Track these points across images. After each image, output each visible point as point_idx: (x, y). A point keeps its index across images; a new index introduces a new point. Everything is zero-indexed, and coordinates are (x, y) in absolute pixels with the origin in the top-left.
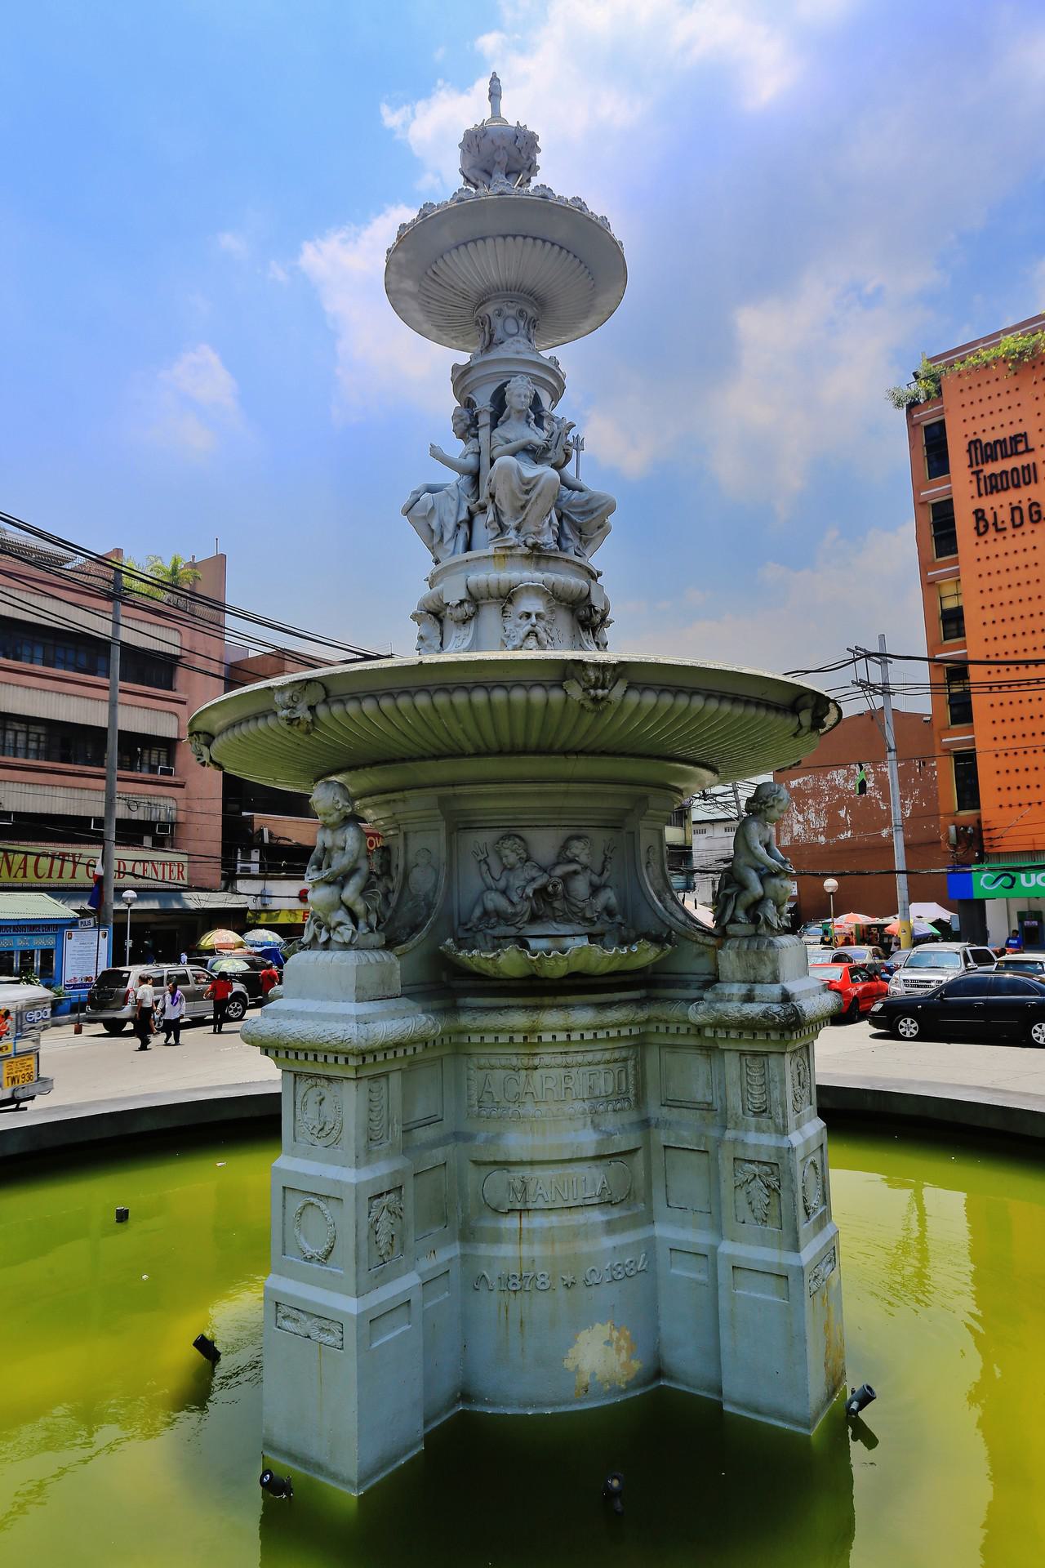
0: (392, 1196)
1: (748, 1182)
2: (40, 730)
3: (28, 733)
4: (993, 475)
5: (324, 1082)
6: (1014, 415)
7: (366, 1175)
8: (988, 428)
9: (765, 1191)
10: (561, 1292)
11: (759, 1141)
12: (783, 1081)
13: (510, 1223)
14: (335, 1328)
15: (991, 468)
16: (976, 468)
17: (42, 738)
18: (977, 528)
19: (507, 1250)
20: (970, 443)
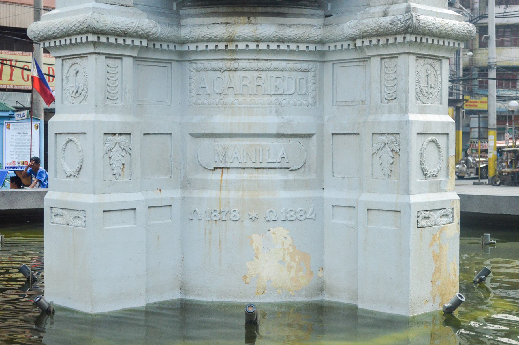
0: (123, 137)
1: (380, 149)
5: (78, 60)
7: (103, 117)
9: (391, 154)
10: (248, 223)
11: (388, 119)
12: (407, 75)
13: (216, 176)
14: (81, 215)
19: (212, 194)
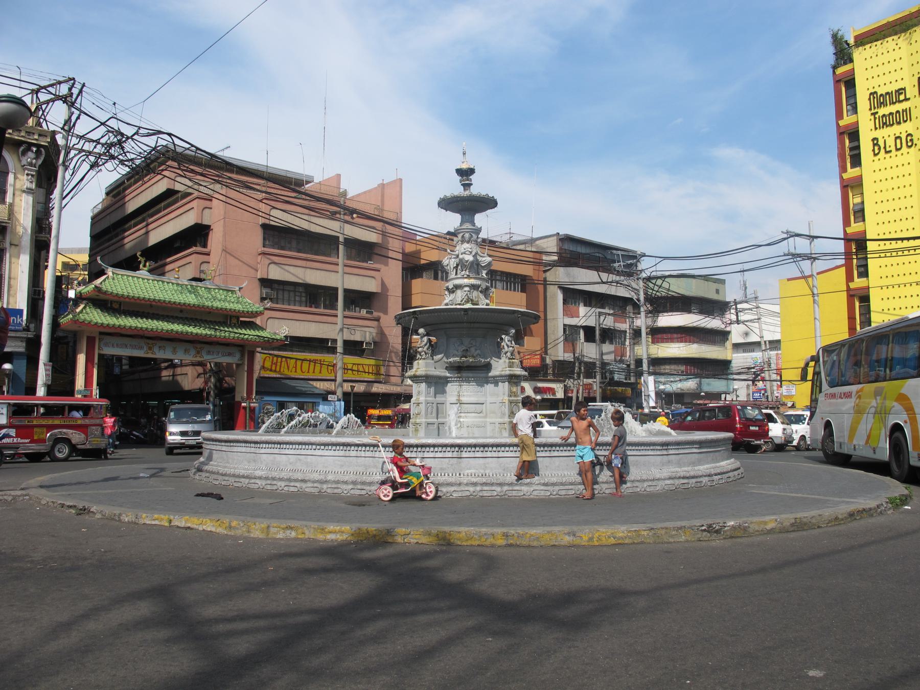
2: (301, 289)
3: (295, 291)
4: (884, 115)
6: (898, 75)
8: (882, 85)
15: (883, 111)
16: (873, 111)
17: (304, 295)
18: (874, 150)
20: (871, 94)
